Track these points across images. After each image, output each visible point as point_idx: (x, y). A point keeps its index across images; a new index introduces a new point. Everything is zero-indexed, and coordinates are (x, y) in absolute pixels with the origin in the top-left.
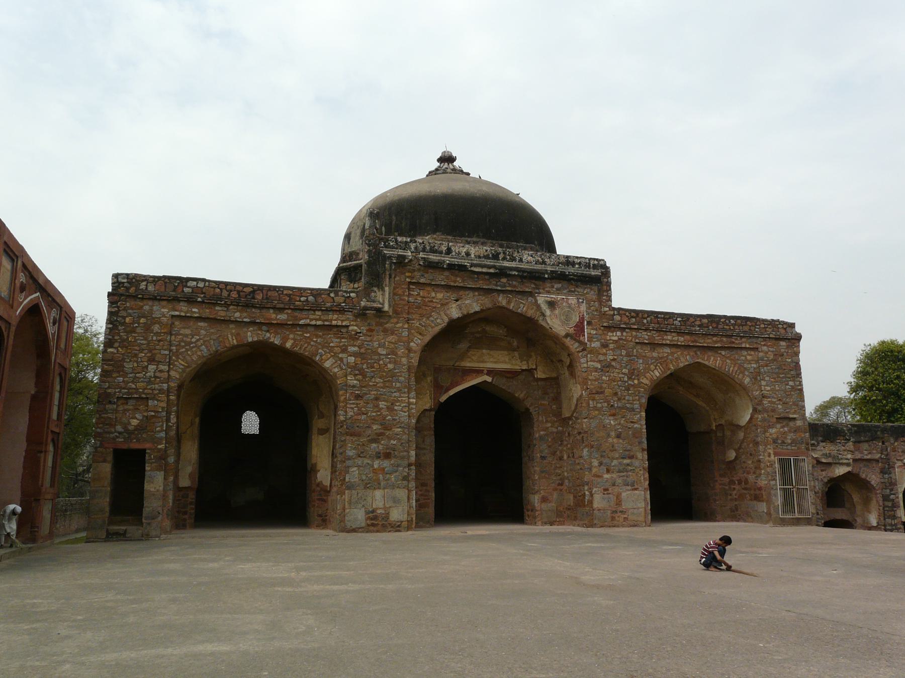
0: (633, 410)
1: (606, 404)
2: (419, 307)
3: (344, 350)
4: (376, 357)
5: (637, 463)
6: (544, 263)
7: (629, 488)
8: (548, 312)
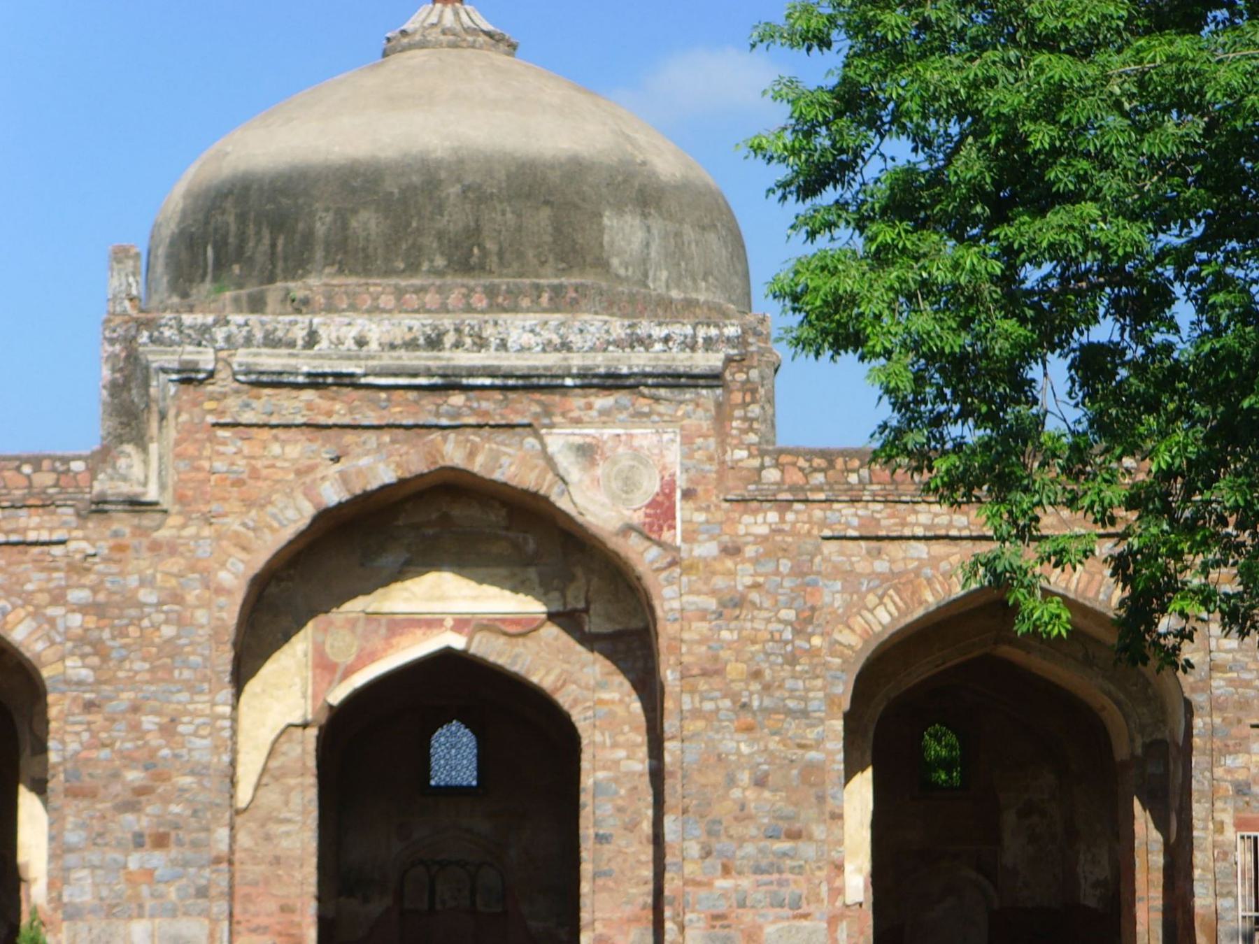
0: (805, 713)
1: (727, 703)
2: (239, 483)
3: (58, 598)
4: (133, 612)
5: (808, 850)
6: (566, 346)
7: (786, 912)
8: (574, 472)
